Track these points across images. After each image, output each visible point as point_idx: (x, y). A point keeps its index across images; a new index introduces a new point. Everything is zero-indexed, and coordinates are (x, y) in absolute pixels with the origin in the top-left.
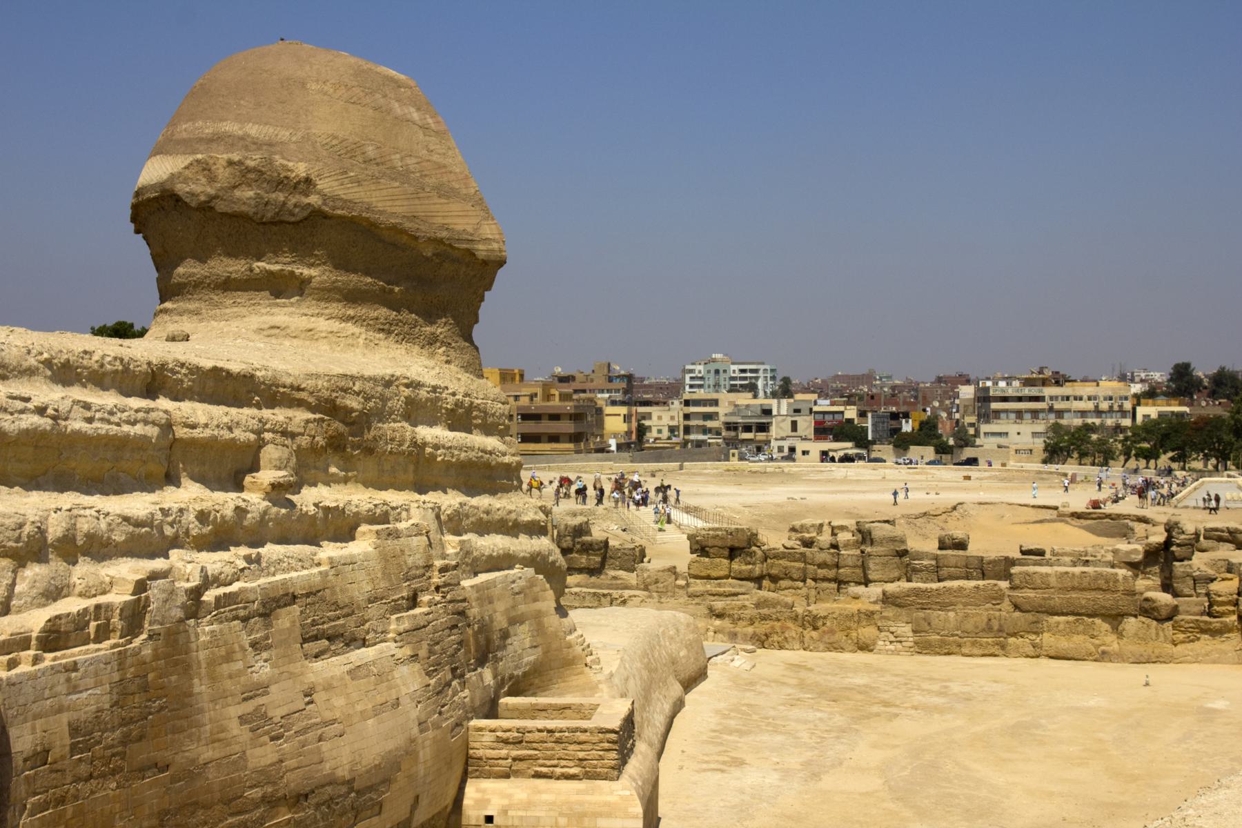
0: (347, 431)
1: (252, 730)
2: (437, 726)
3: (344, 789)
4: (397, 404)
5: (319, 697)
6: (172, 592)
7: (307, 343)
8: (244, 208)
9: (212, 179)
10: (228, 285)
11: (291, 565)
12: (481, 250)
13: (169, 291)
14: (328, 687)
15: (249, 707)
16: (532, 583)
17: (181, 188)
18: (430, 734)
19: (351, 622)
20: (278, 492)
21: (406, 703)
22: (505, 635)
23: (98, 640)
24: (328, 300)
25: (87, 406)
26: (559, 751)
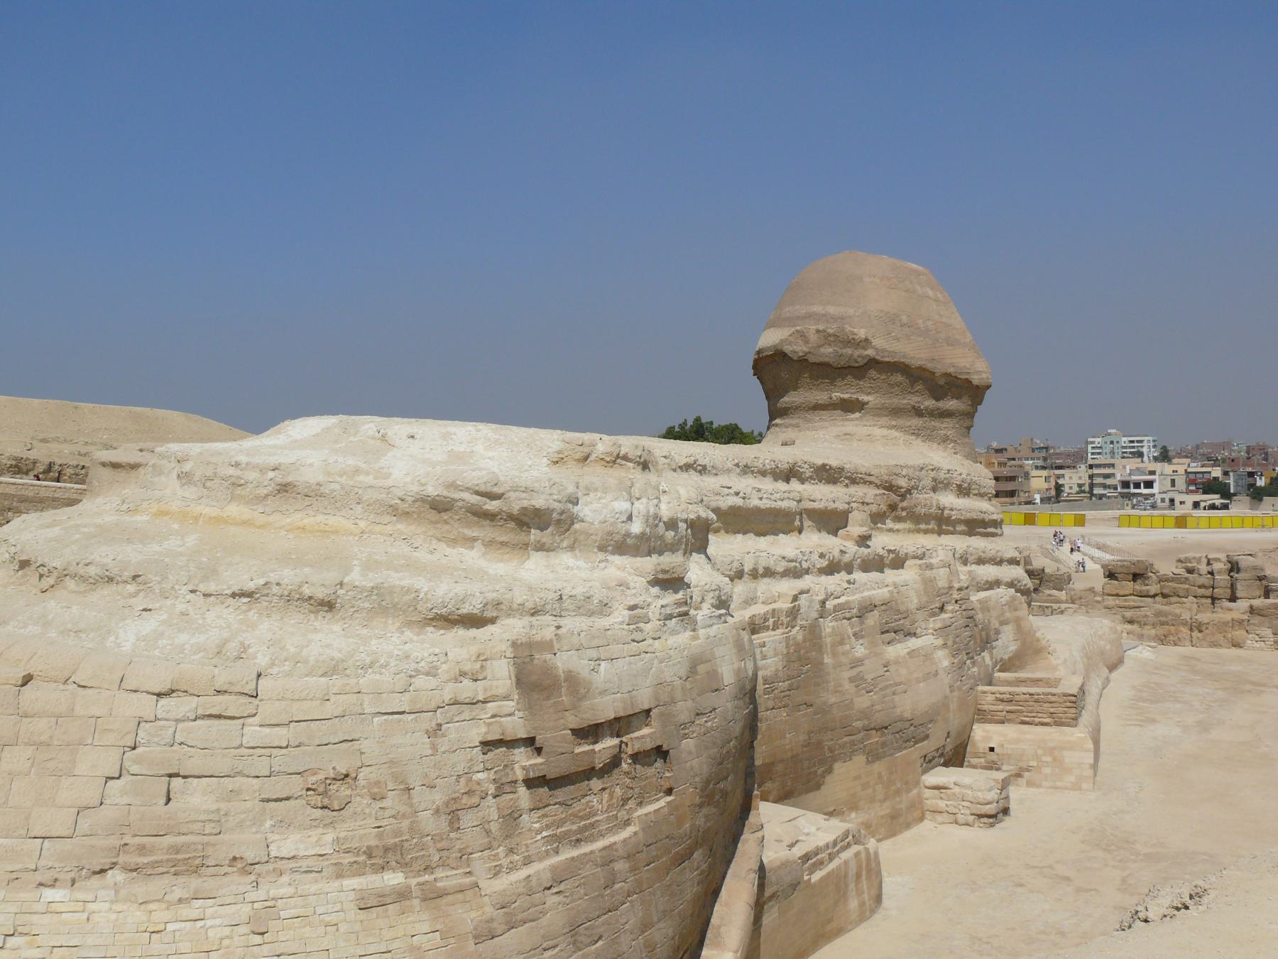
0: (897, 501)
2: (959, 689)
3: (907, 725)
4: (927, 482)
6: (811, 601)
7: (871, 444)
8: (826, 360)
9: (807, 342)
10: (817, 407)
11: (872, 586)
12: (976, 379)
13: (776, 413)
14: (897, 662)
15: (854, 672)
16: (1013, 598)
17: (787, 349)
18: (956, 693)
19: (907, 622)
20: (863, 540)
22: (998, 632)
23: (773, 629)
24: (878, 415)
25: (759, 490)
26: (1037, 707)
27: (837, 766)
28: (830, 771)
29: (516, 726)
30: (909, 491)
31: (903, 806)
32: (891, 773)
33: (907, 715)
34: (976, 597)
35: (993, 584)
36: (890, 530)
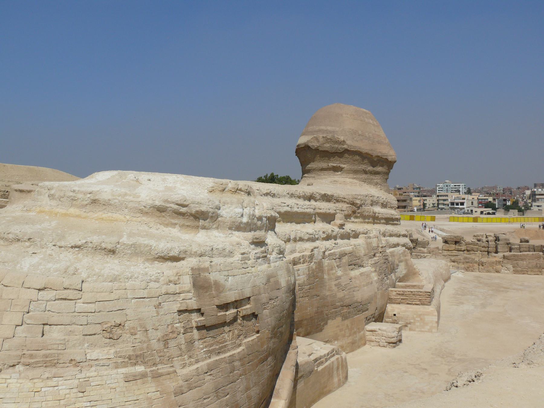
0: (356, 209)
1: (338, 288)
2: (381, 289)
4: (369, 202)
5: (353, 280)
6: (319, 252)
7: (344, 185)
8: (327, 149)
9: (318, 142)
10: (322, 169)
11: (345, 245)
12: (390, 159)
13: (305, 172)
14: (355, 278)
15: (337, 282)
16: (404, 252)
17: (310, 144)
18: (380, 291)
19: (360, 261)
20: (341, 226)
21: (374, 283)
22: (398, 266)
23: (303, 264)
24: (348, 173)
25: (297, 204)
26: (414, 297)
27: (329, 321)
28: (326, 324)
29: (193, 304)
30: (361, 206)
31: (357, 339)
32: (352, 325)
33: (359, 300)
34: (389, 251)
35: (396, 245)
36: (353, 222)
